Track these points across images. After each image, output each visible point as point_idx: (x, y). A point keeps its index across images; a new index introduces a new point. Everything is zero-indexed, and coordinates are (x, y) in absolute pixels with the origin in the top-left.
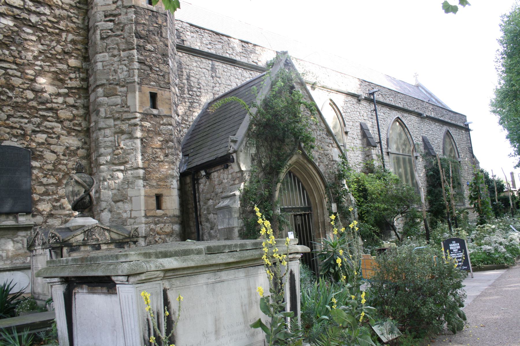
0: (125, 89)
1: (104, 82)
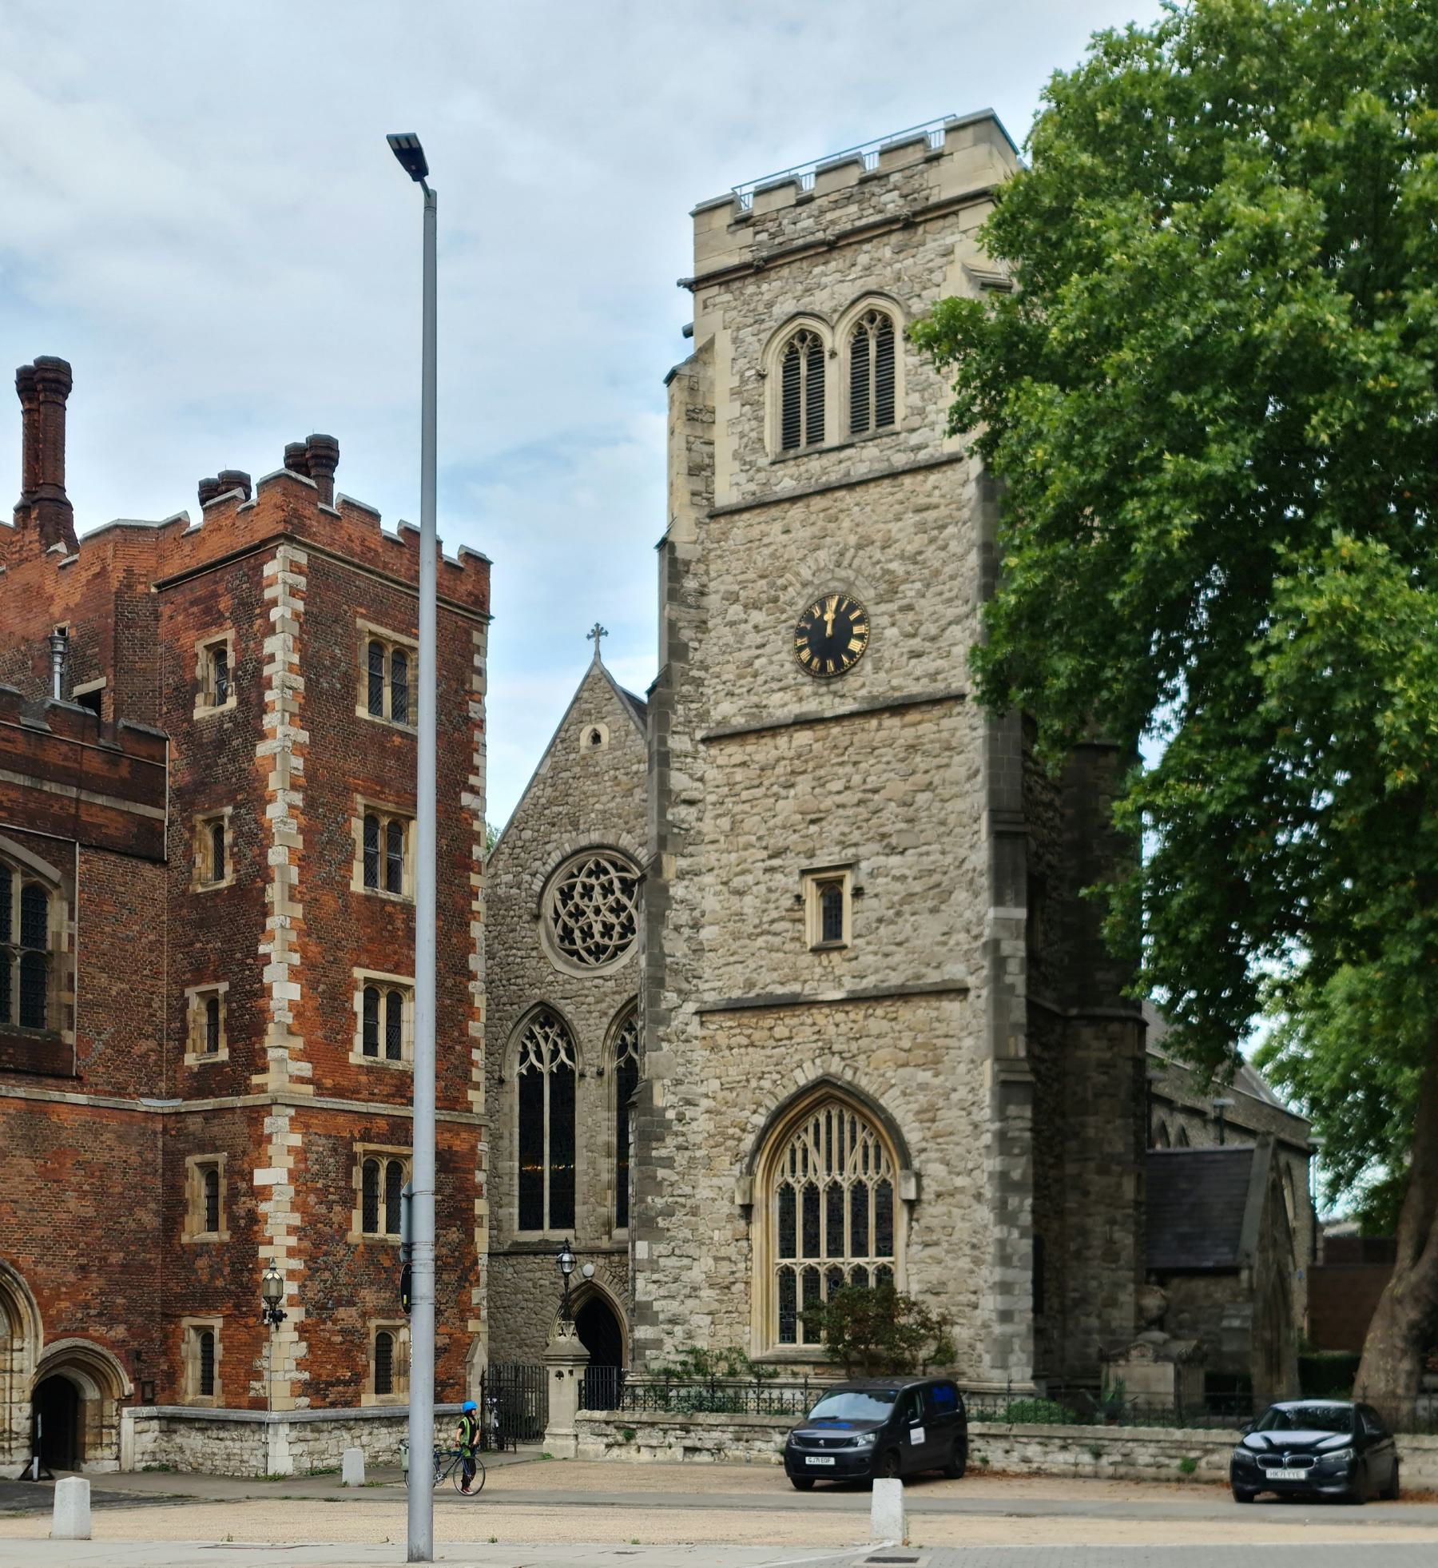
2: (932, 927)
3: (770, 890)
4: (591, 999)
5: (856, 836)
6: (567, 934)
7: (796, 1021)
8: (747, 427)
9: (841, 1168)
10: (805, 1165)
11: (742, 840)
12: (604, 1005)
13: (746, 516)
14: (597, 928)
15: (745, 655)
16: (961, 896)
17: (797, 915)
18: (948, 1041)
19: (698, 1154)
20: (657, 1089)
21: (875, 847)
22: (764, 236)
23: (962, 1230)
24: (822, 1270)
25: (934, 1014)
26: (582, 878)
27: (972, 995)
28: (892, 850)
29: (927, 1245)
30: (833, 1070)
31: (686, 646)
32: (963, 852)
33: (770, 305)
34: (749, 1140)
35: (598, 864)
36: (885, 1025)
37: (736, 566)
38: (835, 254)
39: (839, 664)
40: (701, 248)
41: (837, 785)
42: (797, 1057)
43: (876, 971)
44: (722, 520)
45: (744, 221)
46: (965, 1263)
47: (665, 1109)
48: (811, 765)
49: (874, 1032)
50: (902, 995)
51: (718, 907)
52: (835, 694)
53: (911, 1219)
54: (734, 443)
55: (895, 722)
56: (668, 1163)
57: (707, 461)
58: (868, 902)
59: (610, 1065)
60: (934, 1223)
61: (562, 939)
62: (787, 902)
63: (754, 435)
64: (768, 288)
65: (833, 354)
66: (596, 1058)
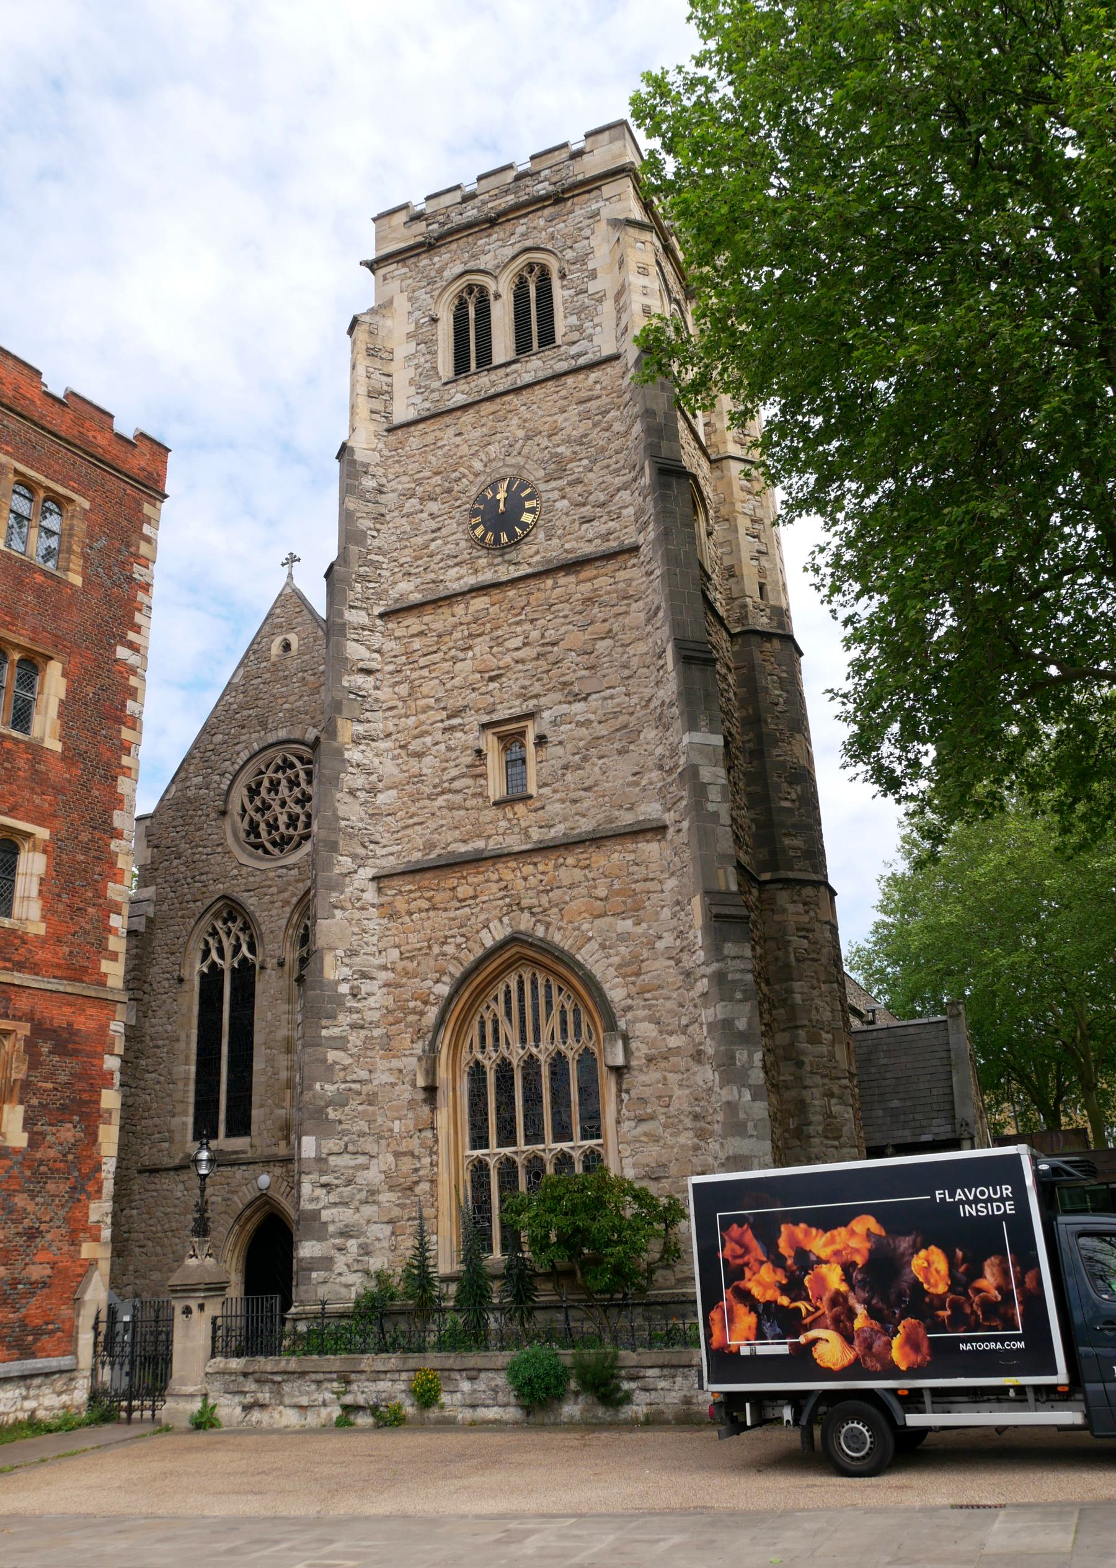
0: (830, 1036)
1: (806, 1022)
2: (621, 769)
3: (449, 749)
4: (274, 890)
5: (537, 688)
6: (253, 829)
7: (481, 878)
8: (422, 360)
9: (537, 1039)
10: (496, 1039)
11: (419, 703)
12: (286, 895)
13: (421, 426)
14: (283, 819)
15: (420, 540)
16: (650, 734)
17: (478, 771)
18: (649, 885)
19: (376, 1033)
20: (329, 960)
21: (558, 696)
22: (435, 226)
23: (681, 1098)
24: (520, 1160)
25: (631, 857)
26: (270, 773)
27: (671, 830)
28: (577, 698)
29: (641, 1120)
30: (522, 927)
31: (364, 534)
32: (647, 692)
33: (440, 271)
34: (433, 1013)
35: (285, 760)
36: (578, 874)
37: (412, 467)
38: (496, 229)
39: (512, 535)
40: (380, 240)
41: (517, 642)
42: (482, 917)
43: (565, 819)
44: (399, 432)
45: (418, 217)
46: (686, 1139)
47: (337, 983)
48: (488, 626)
49: (566, 882)
50: (596, 840)
51: (396, 771)
52: (510, 563)
53: (620, 1090)
54: (411, 373)
55: (572, 579)
56: (340, 1043)
57: (385, 388)
58: (552, 750)
59: (292, 956)
60: (647, 1092)
61: (248, 834)
62: (468, 758)
63: (428, 365)
64: (438, 259)
65: (497, 296)
66: (275, 947)
